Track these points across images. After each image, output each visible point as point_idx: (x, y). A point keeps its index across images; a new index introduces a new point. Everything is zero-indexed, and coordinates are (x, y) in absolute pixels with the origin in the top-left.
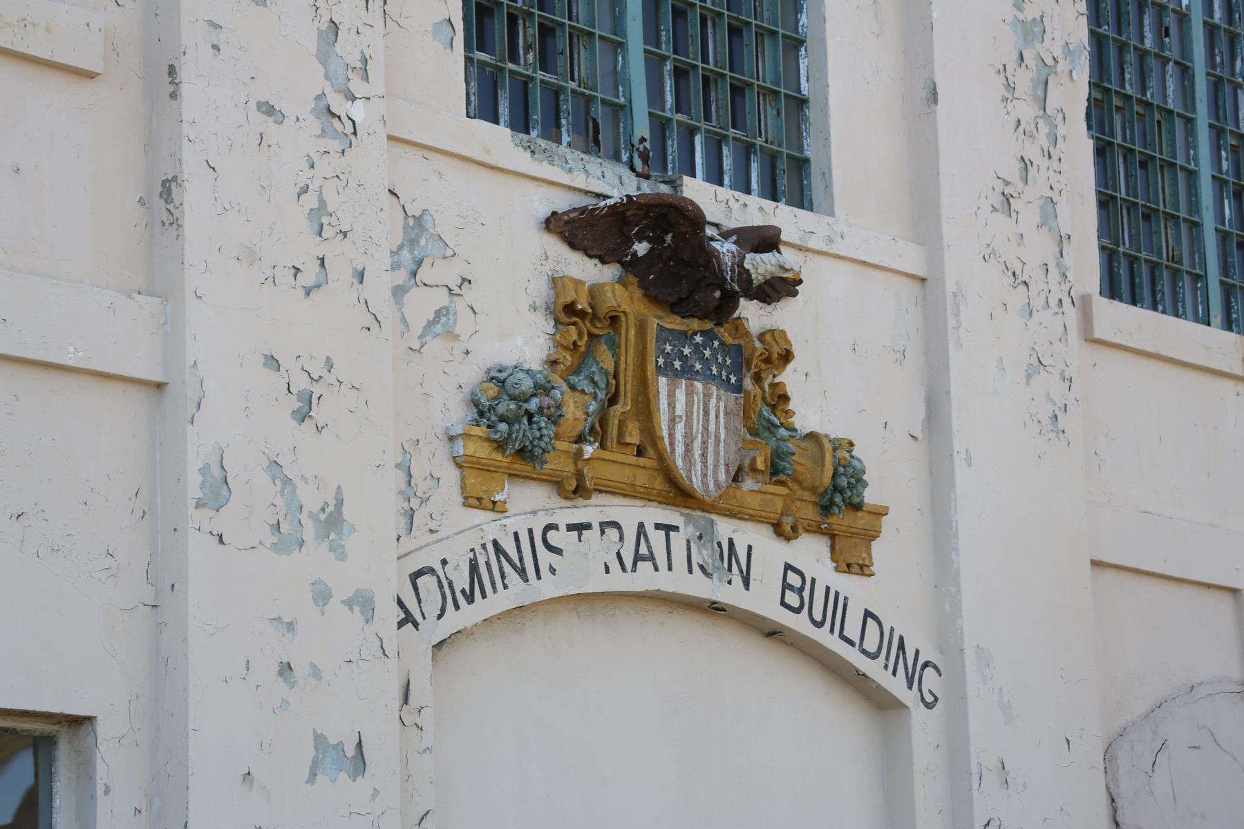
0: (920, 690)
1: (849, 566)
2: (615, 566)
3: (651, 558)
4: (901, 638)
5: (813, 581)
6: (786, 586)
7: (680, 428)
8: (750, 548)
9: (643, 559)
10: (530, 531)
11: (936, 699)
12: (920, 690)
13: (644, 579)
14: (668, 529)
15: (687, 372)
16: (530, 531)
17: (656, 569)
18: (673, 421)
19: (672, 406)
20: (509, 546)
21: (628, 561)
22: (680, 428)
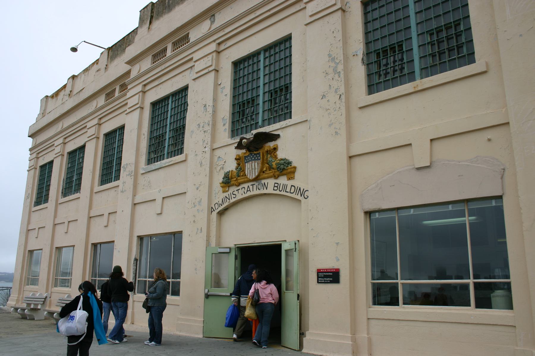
0: (304, 196)
1: (289, 178)
4: (300, 188)
5: (280, 184)
6: (275, 186)
8: (268, 183)
11: (308, 197)
12: (304, 196)
13: (249, 194)
14: (253, 185)
16: (231, 193)
17: (250, 192)
20: (228, 197)
21: (246, 193)
22: (249, 170)
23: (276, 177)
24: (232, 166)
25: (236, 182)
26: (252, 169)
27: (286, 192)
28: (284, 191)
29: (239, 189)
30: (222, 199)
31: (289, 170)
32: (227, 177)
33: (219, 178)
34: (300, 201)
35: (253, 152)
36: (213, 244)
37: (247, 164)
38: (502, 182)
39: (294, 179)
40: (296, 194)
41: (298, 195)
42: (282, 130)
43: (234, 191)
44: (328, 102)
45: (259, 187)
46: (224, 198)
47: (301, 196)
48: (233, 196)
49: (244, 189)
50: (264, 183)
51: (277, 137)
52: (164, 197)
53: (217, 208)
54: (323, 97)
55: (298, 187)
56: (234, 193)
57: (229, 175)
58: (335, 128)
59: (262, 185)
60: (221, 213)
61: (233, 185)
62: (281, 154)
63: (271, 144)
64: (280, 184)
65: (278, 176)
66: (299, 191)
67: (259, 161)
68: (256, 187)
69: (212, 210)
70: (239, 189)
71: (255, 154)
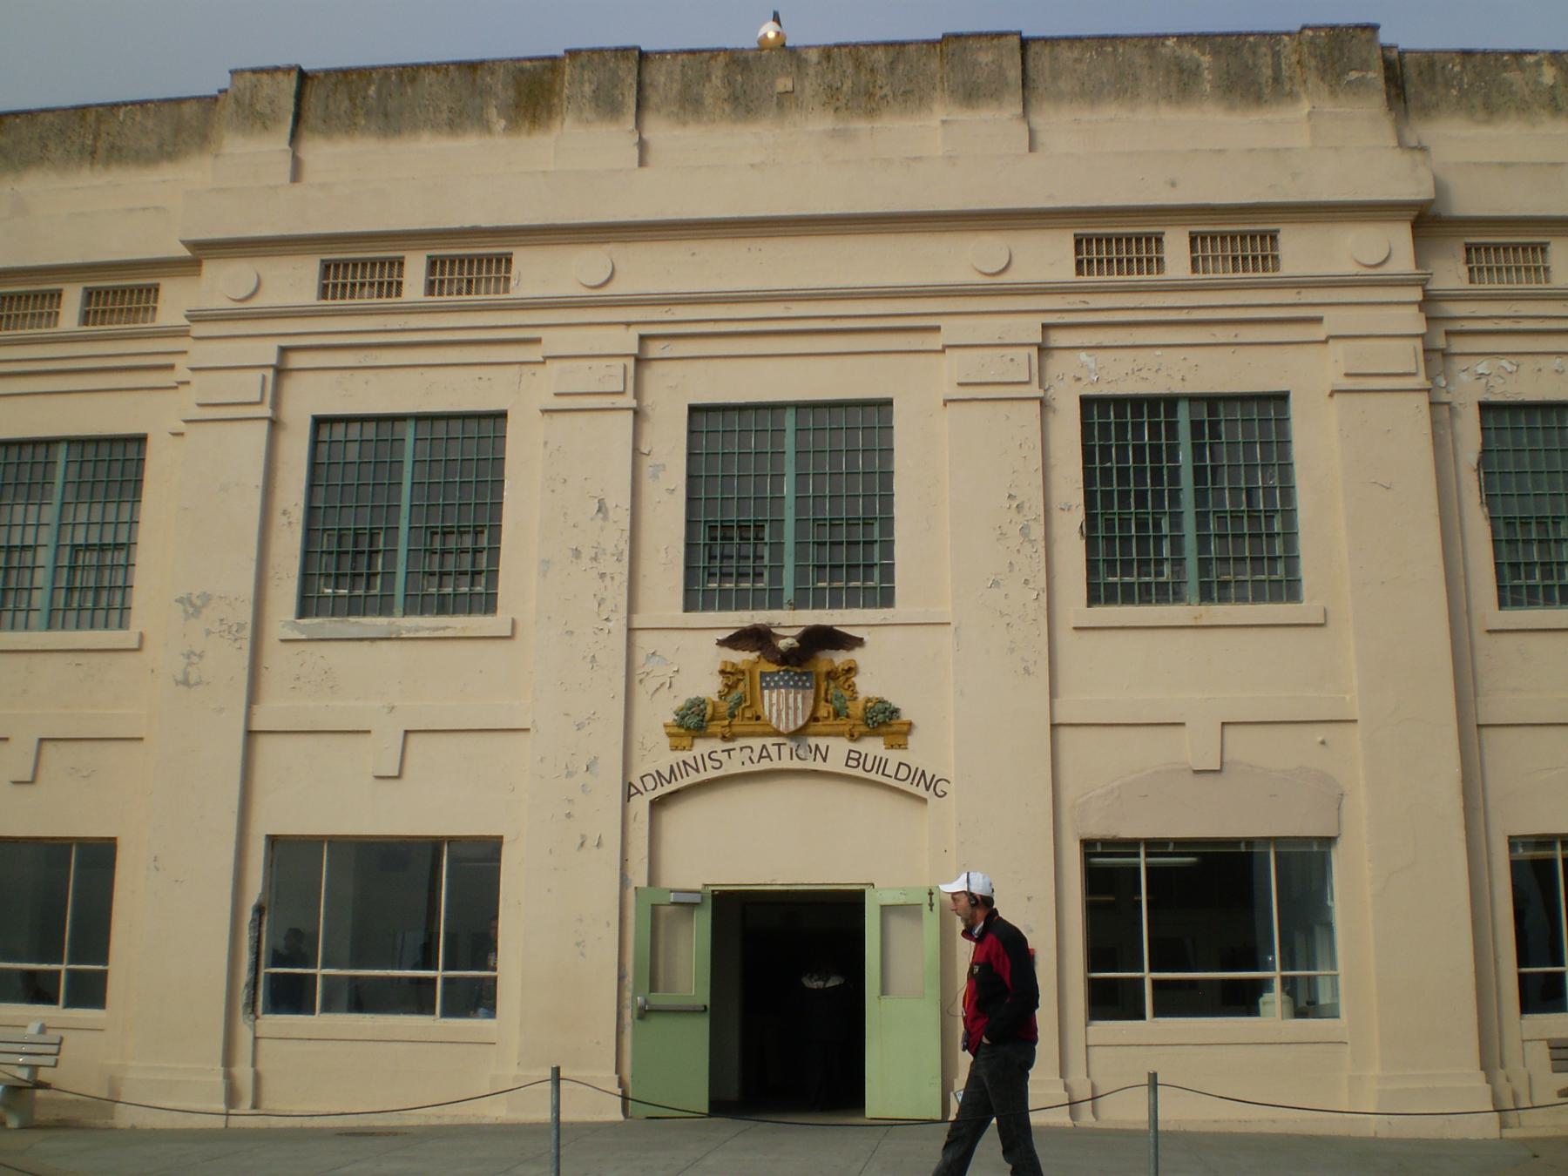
1: (892, 746)
2: (748, 762)
3: (769, 756)
5: (866, 755)
6: (849, 758)
7: (775, 708)
8: (828, 747)
9: (765, 757)
10: (702, 756)
13: (765, 765)
14: (779, 745)
15: (777, 687)
16: (702, 756)
17: (771, 760)
18: (771, 705)
19: (770, 700)
21: (755, 760)
22: (775, 708)
23: (853, 737)
24: (709, 687)
25: (727, 730)
26: (788, 708)
27: (883, 774)
28: (877, 772)
29: (734, 749)
30: (672, 766)
31: (895, 729)
32: (698, 715)
33: (657, 713)
34: (924, 801)
35: (792, 666)
36: (639, 877)
37: (766, 692)
38: (1339, 813)
39: (906, 748)
40: (912, 784)
41: (917, 785)
42: (870, 629)
43: (716, 752)
44: (1006, 598)
45: (801, 752)
46: (678, 764)
47: (927, 788)
48: (709, 763)
49: (750, 750)
50: (817, 746)
51: (853, 642)
52: (407, 729)
53: (653, 787)
54: (995, 583)
55: (917, 769)
56: (712, 756)
57: (705, 709)
58: (1023, 659)
59: (808, 748)
60: (657, 804)
61: (713, 736)
62: (868, 686)
63: (840, 658)
64: (866, 755)
65: (862, 735)
66: (920, 779)
67: (808, 692)
68: (789, 752)
69: (628, 792)
70: (734, 749)
71: (796, 673)
